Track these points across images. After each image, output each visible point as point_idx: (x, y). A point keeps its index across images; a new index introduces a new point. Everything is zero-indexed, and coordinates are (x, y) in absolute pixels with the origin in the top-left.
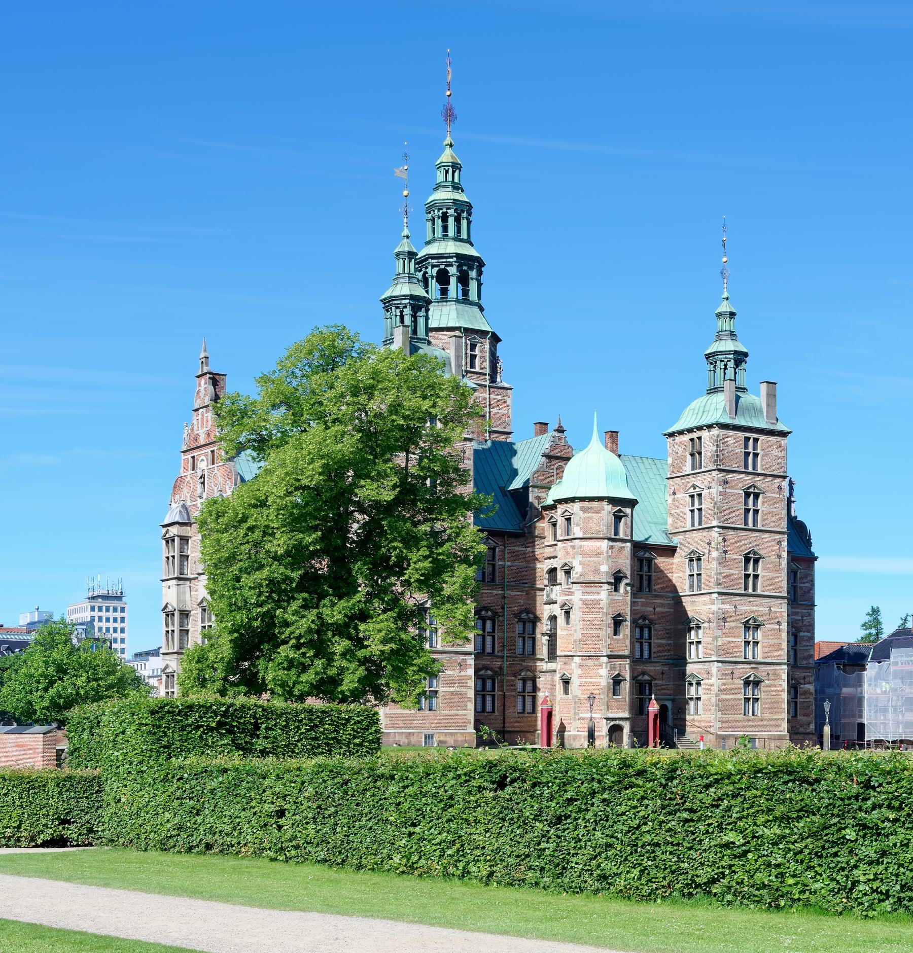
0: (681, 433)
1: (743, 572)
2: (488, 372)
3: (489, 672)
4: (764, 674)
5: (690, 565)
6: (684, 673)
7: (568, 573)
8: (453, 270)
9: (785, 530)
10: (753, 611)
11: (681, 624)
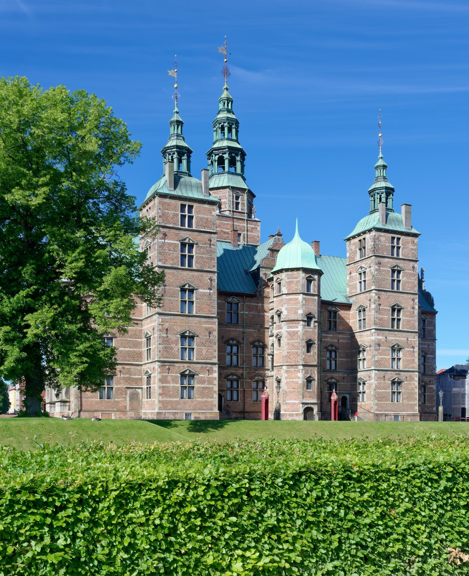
0: (354, 237)
1: (391, 317)
2: (246, 211)
3: (235, 377)
4: (404, 378)
5: (359, 315)
6: (356, 378)
7: (279, 316)
8: (226, 156)
9: (417, 292)
10: (397, 340)
11: (354, 349)
